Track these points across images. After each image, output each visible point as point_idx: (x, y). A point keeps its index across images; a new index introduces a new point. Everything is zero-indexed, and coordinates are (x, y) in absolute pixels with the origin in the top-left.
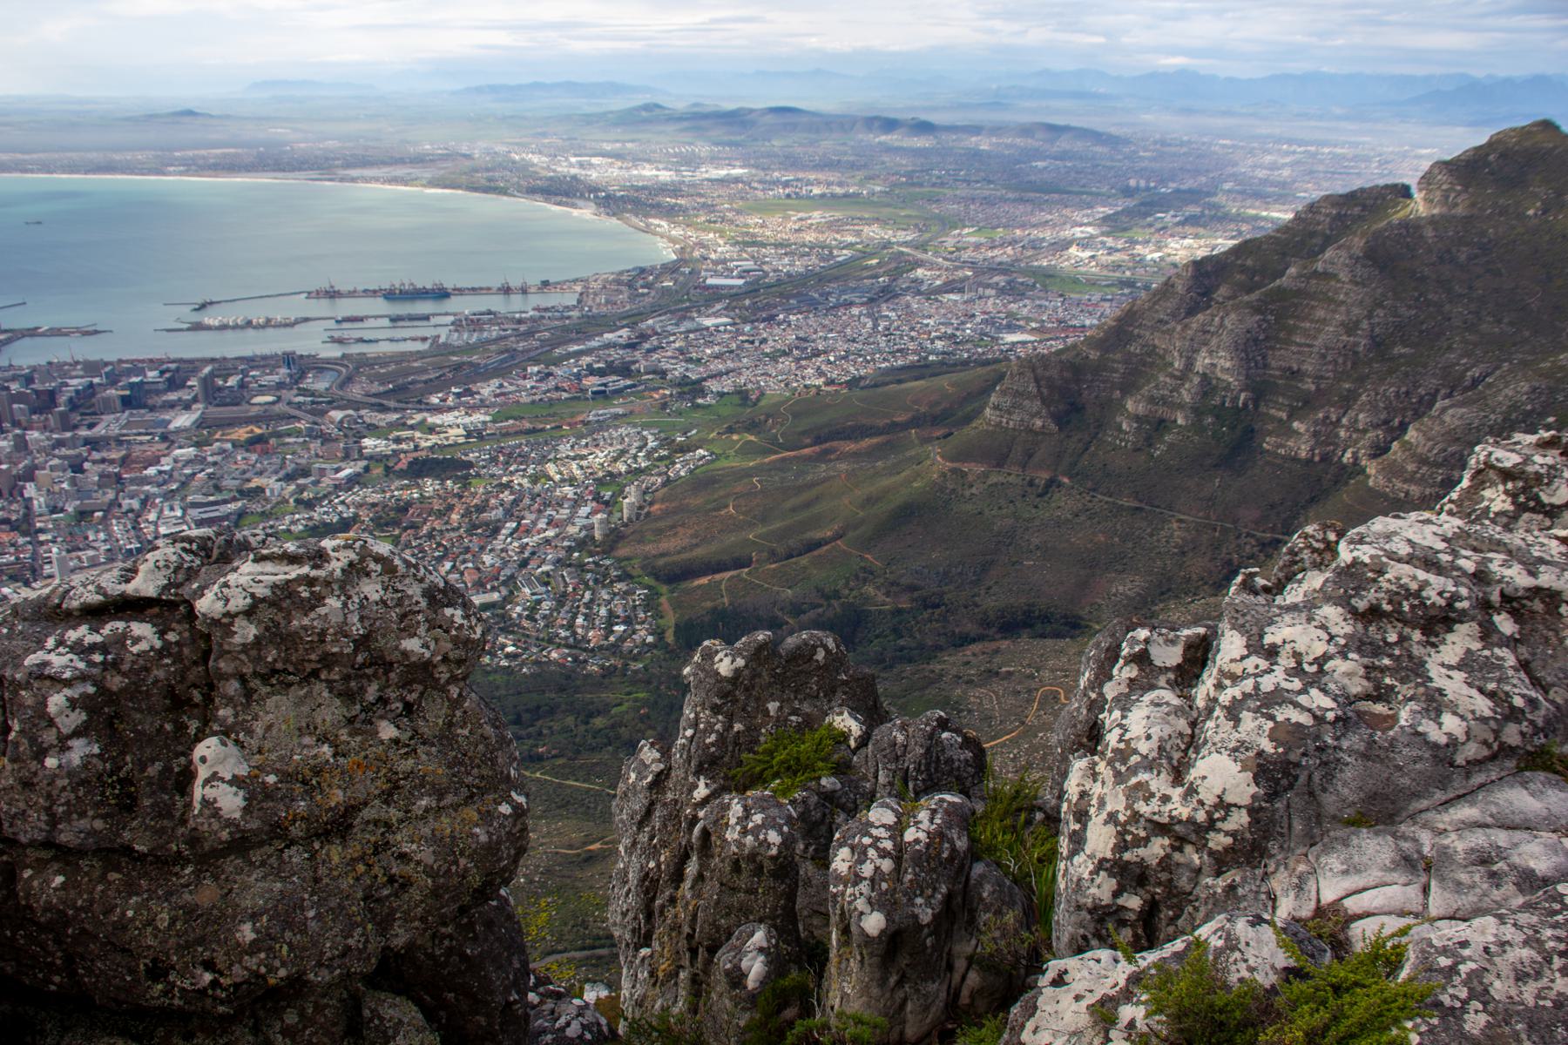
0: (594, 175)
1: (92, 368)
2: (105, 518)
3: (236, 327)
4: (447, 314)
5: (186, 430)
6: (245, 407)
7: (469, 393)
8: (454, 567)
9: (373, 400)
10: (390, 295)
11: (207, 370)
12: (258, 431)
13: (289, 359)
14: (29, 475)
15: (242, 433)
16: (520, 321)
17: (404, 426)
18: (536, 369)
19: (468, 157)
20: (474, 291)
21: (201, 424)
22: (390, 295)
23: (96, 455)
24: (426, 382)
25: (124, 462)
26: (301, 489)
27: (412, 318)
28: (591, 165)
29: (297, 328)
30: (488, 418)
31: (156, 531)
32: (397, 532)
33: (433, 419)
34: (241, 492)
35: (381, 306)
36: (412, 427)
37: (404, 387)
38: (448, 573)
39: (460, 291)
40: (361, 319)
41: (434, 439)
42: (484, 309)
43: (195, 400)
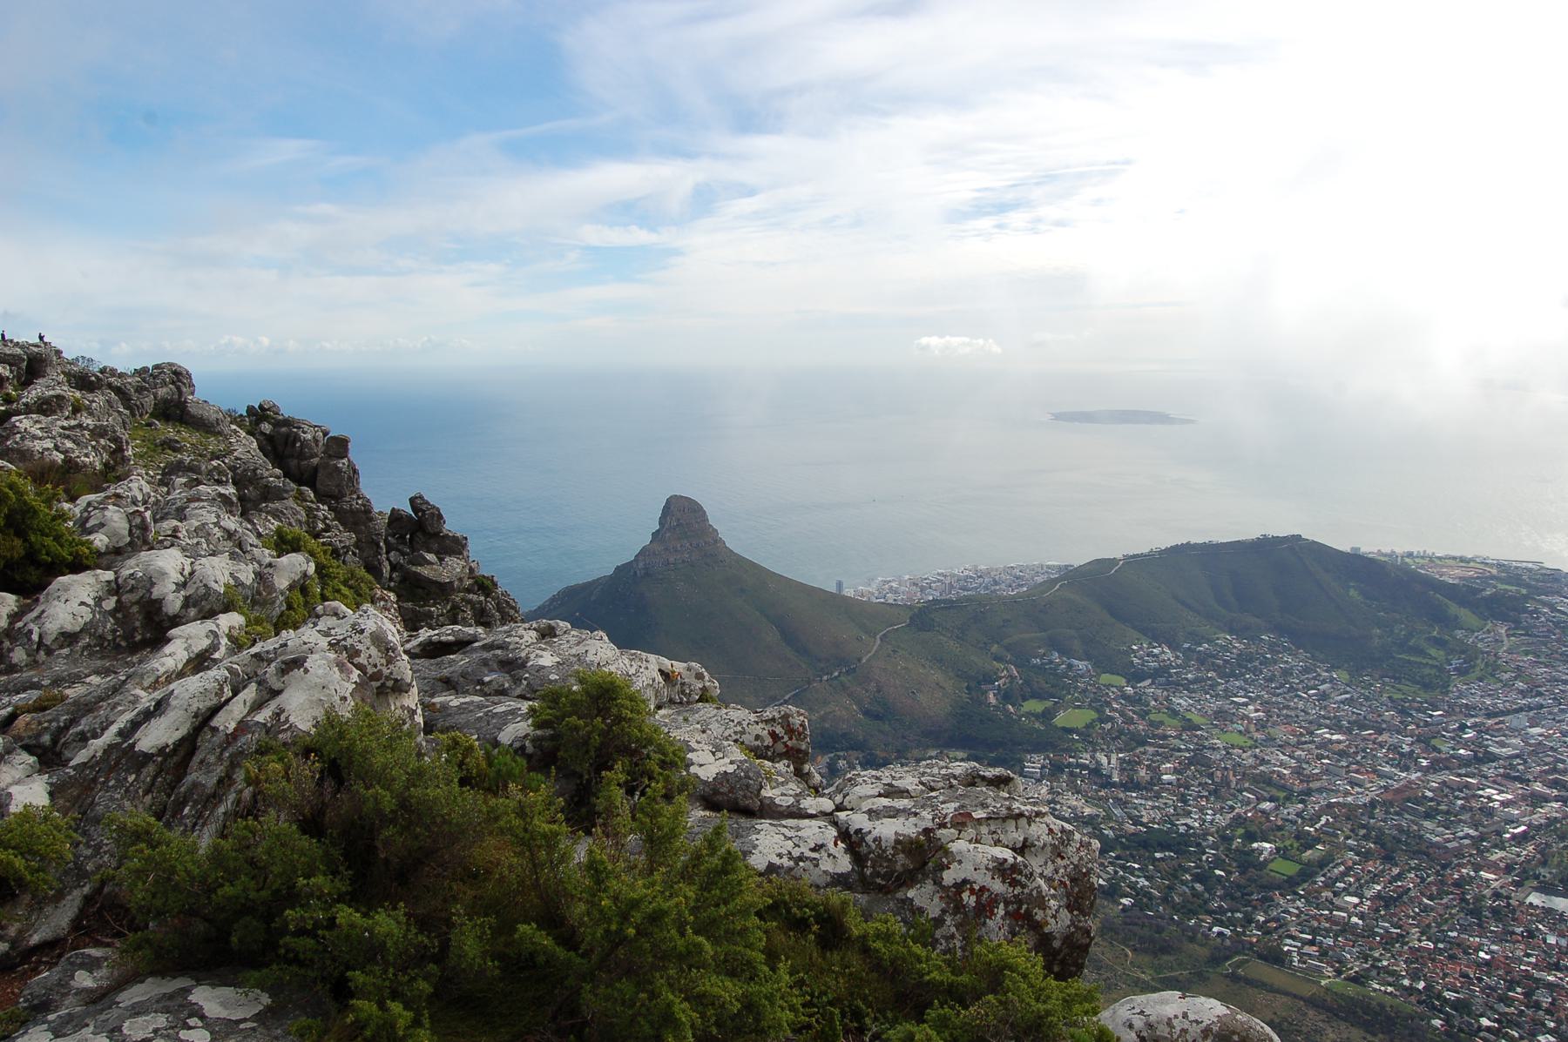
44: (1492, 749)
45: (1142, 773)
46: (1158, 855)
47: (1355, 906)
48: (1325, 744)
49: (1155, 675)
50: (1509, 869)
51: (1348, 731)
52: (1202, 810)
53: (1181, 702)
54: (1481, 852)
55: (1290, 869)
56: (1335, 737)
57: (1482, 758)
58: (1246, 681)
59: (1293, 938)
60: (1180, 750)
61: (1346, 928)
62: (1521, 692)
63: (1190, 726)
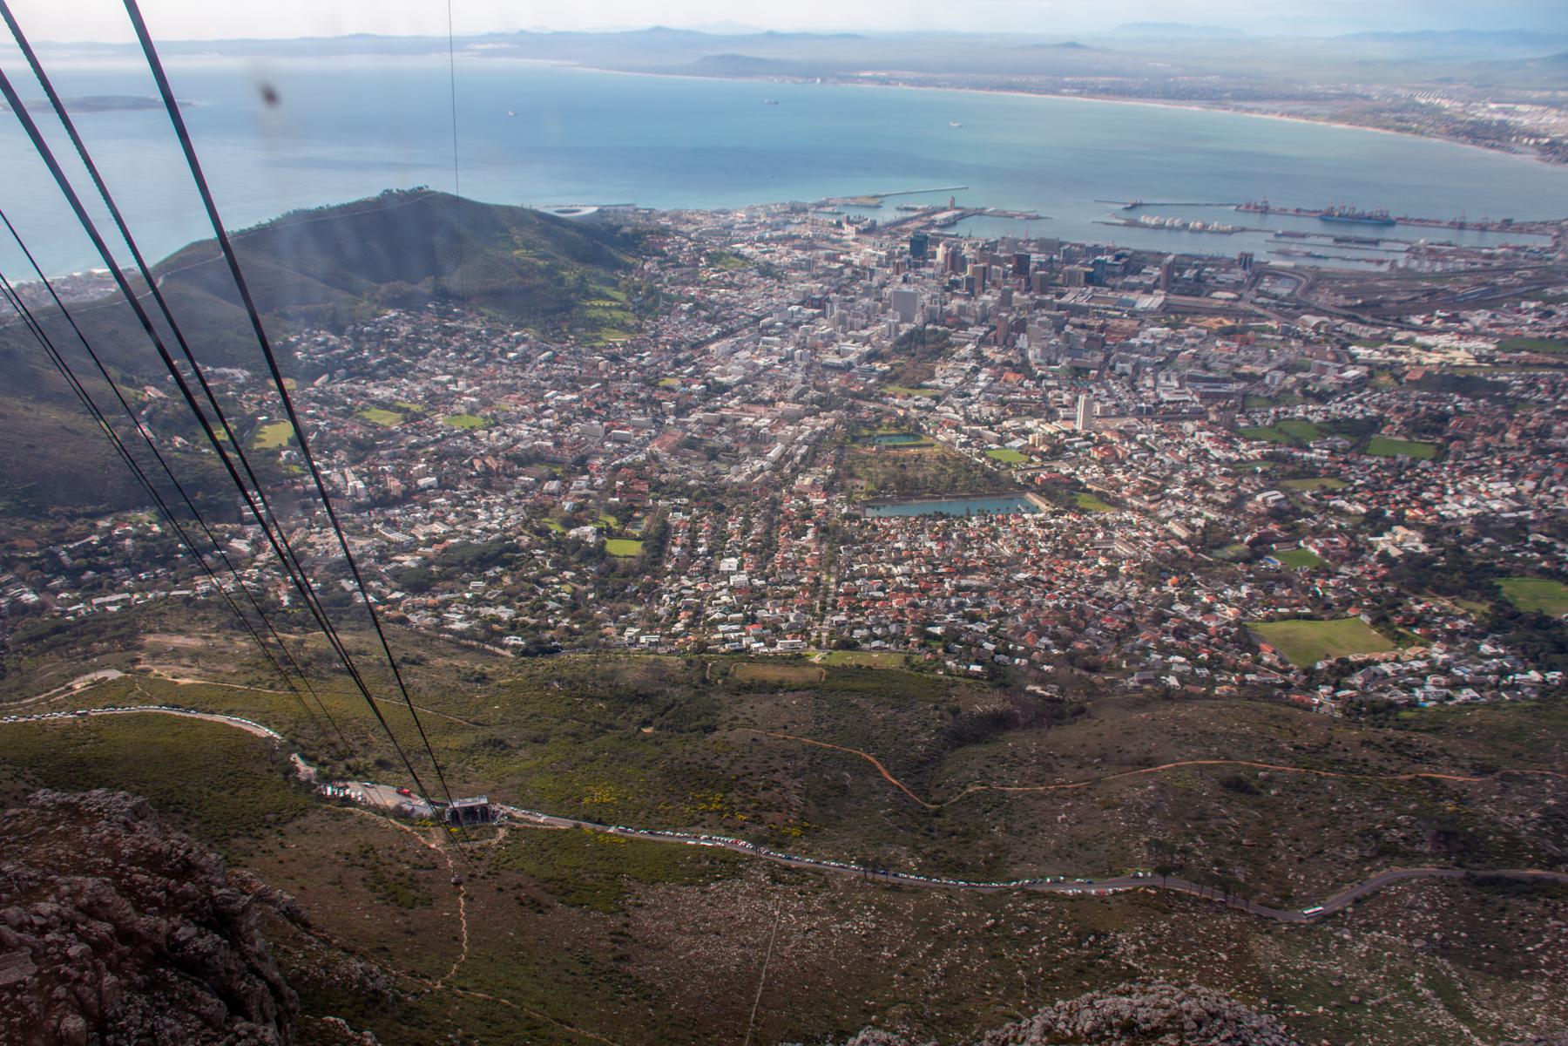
0: (1526, 122)
1: (1045, 245)
2: (1098, 378)
3: (1171, 228)
4: (1396, 241)
5: (1152, 312)
6: (1207, 300)
7: (1455, 318)
8: (1538, 486)
9: (1347, 313)
10: (1327, 217)
11: (1170, 258)
12: (1227, 323)
13: (1246, 261)
14: (1021, 326)
15: (1213, 322)
16: (1490, 257)
17: (1389, 340)
18: (1532, 305)
19: (1367, 98)
20: (1421, 222)
21: (1166, 308)
22: (1327, 217)
23: (1073, 320)
24: (1399, 302)
25: (1102, 328)
26: (1305, 383)
27: (1359, 241)
28: (1519, 114)
29: (1235, 237)
30: (1491, 347)
31: (1157, 396)
32: (1439, 441)
33: (1429, 340)
34: (1234, 374)
35: (1312, 225)
36: (1400, 343)
37: (1379, 307)
38: (1533, 492)
39: (1405, 221)
40: (1303, 236)
41: (1436, 358)
42: (1443, 240)
43: (1155, 286)
44: (718, 379)
45: (396, 483)
46: (490, 573)
47: (740, 567)
48: (562, 407)
49: (329, 368)
50: (828, 489)
51: (575, 389)
52: (488, 507)
53: (381, 393)
54: (788, 481)
55: (634, 548)
56: (568, 397)
57: (716, 389)
58: (435, 356)
59: (723, 621)
60: (418, 446)
61: (758, 596)
62: (708, 319)
63: (412, 418)
